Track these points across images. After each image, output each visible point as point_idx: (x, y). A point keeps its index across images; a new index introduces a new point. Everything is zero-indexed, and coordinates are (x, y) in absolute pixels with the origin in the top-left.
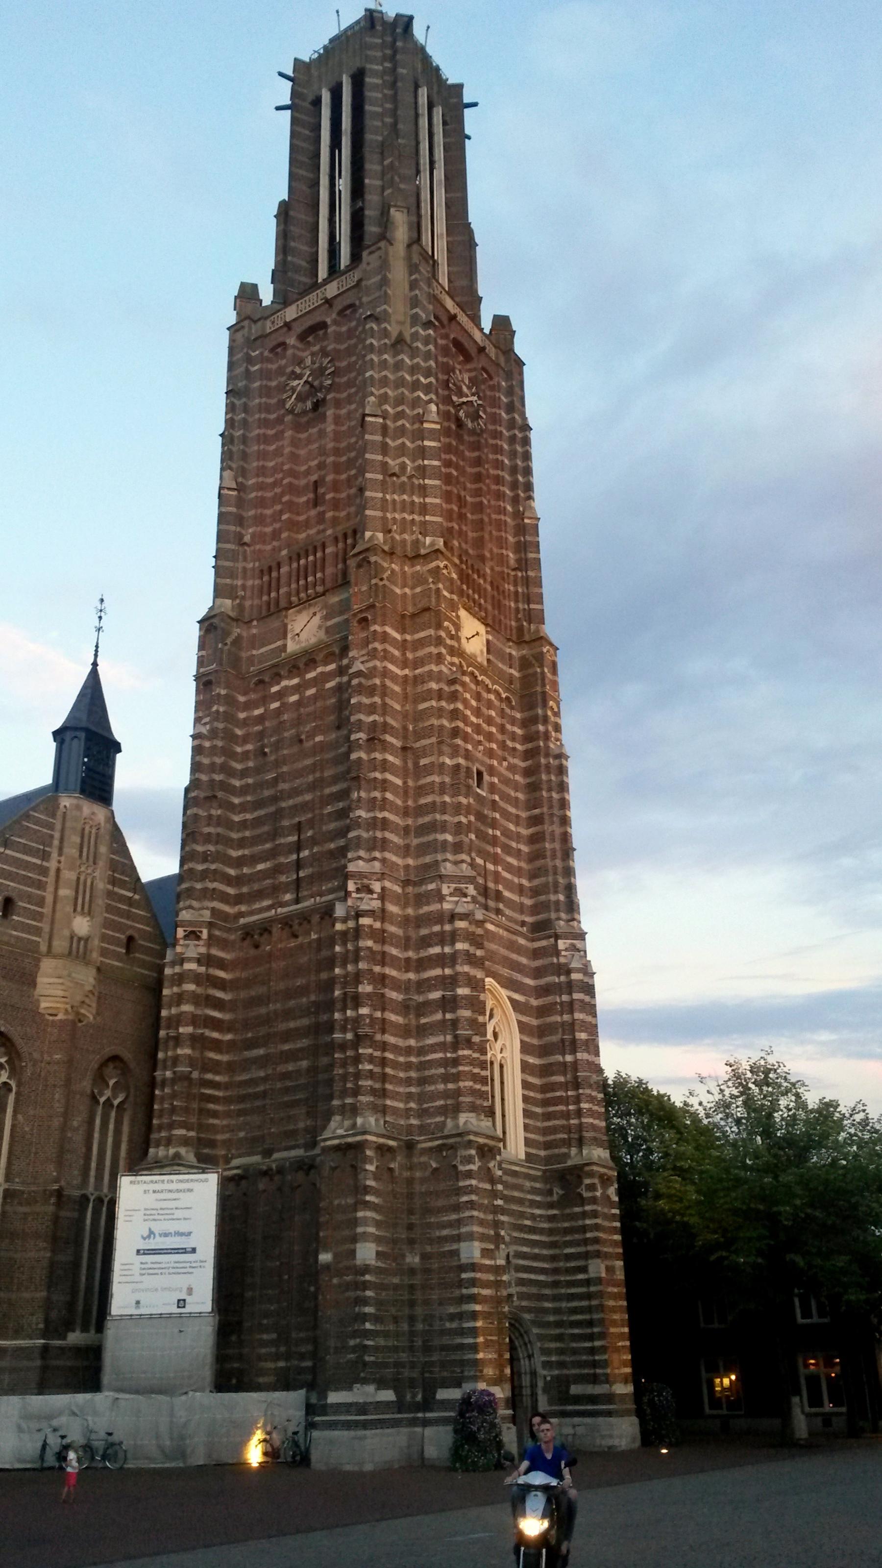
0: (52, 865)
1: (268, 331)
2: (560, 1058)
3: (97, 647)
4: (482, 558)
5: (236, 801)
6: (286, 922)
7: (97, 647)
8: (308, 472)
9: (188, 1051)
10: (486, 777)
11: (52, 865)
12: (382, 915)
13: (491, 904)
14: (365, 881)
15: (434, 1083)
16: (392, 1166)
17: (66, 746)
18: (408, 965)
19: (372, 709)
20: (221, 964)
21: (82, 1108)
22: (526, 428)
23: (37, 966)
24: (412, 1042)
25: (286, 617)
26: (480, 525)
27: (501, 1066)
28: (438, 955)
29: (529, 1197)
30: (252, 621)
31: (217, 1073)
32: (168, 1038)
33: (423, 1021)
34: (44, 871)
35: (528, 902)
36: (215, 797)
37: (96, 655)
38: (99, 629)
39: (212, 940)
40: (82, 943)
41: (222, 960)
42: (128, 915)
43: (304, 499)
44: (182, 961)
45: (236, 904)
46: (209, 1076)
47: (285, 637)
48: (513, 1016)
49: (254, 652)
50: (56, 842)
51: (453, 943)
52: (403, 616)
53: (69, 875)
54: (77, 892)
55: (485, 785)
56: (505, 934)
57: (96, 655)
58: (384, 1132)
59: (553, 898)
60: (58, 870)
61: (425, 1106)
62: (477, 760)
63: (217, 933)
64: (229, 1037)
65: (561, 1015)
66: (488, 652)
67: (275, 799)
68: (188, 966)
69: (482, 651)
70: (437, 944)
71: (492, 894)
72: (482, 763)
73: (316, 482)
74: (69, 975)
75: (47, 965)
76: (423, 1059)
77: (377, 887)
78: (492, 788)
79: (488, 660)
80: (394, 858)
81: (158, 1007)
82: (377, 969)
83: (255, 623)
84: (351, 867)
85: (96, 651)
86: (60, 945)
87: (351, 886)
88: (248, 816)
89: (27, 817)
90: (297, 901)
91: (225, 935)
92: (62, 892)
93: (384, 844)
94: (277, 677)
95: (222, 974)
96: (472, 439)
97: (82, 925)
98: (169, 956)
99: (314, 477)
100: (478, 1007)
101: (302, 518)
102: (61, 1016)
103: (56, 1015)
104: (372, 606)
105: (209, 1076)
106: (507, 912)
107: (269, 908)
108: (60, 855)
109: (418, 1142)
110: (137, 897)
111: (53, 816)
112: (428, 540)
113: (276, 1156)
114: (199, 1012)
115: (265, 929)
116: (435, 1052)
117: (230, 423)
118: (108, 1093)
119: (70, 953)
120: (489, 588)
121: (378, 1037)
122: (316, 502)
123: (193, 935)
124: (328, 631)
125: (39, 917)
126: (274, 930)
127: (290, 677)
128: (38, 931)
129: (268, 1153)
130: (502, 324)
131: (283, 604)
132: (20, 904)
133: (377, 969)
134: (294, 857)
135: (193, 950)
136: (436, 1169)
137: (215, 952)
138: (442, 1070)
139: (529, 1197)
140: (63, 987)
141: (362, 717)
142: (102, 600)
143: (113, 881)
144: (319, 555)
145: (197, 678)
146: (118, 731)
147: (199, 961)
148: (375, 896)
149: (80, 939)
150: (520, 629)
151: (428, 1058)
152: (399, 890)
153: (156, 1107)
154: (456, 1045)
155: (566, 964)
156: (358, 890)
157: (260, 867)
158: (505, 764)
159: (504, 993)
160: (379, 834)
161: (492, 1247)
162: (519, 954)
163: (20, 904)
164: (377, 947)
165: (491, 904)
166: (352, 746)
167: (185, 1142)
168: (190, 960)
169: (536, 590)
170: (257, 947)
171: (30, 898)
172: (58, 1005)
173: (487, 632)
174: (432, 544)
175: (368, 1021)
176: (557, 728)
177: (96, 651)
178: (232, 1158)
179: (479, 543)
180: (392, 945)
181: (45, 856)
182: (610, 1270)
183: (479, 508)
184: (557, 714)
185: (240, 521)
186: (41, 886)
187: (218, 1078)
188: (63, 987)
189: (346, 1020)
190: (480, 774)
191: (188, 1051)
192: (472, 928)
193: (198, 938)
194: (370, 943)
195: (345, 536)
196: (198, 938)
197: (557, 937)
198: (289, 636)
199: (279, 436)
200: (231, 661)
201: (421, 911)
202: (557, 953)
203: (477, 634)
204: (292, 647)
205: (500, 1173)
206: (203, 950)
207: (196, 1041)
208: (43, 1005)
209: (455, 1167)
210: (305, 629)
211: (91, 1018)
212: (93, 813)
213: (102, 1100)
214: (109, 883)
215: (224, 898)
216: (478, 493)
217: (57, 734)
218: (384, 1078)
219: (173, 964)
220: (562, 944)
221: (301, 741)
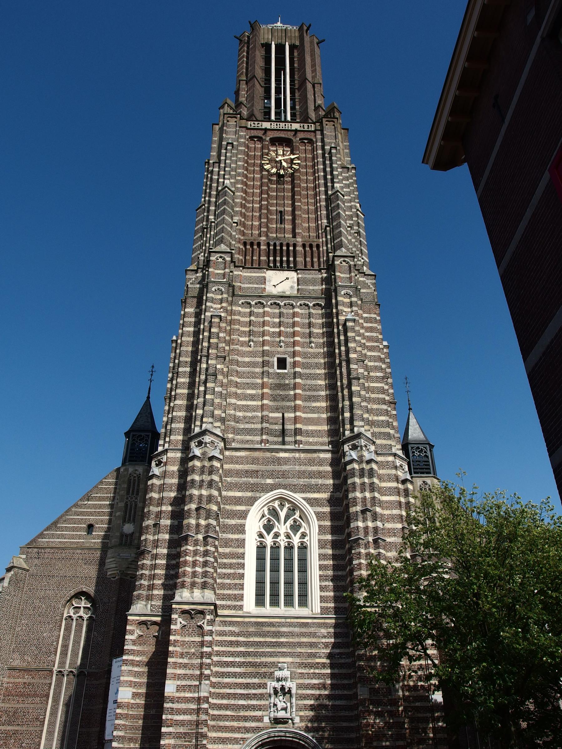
3: (150, 389)
7: (150, 389)
10: (289, 360)
29: (324, 640)
37: (149, 393)
54: (126, 512)
56: (302, 455)
57: (149, 393)
58: (149, 612)
74: (119, 555)
85: (149, 391)
89: (101, 482)
102: (117, 578)
132: (97, 526)
139: (324, 640)
140: (115, 562)
142: (153, 367)
149: (127, 536)
159: (298, 497)
161: (197, 683)
162: (321, 465)
163: (97, 526)
172: (115, 572)
173: (298, 274)
177: (149, 391)
188: (115, 562)
208: (109, 573)
212: (136, 470)
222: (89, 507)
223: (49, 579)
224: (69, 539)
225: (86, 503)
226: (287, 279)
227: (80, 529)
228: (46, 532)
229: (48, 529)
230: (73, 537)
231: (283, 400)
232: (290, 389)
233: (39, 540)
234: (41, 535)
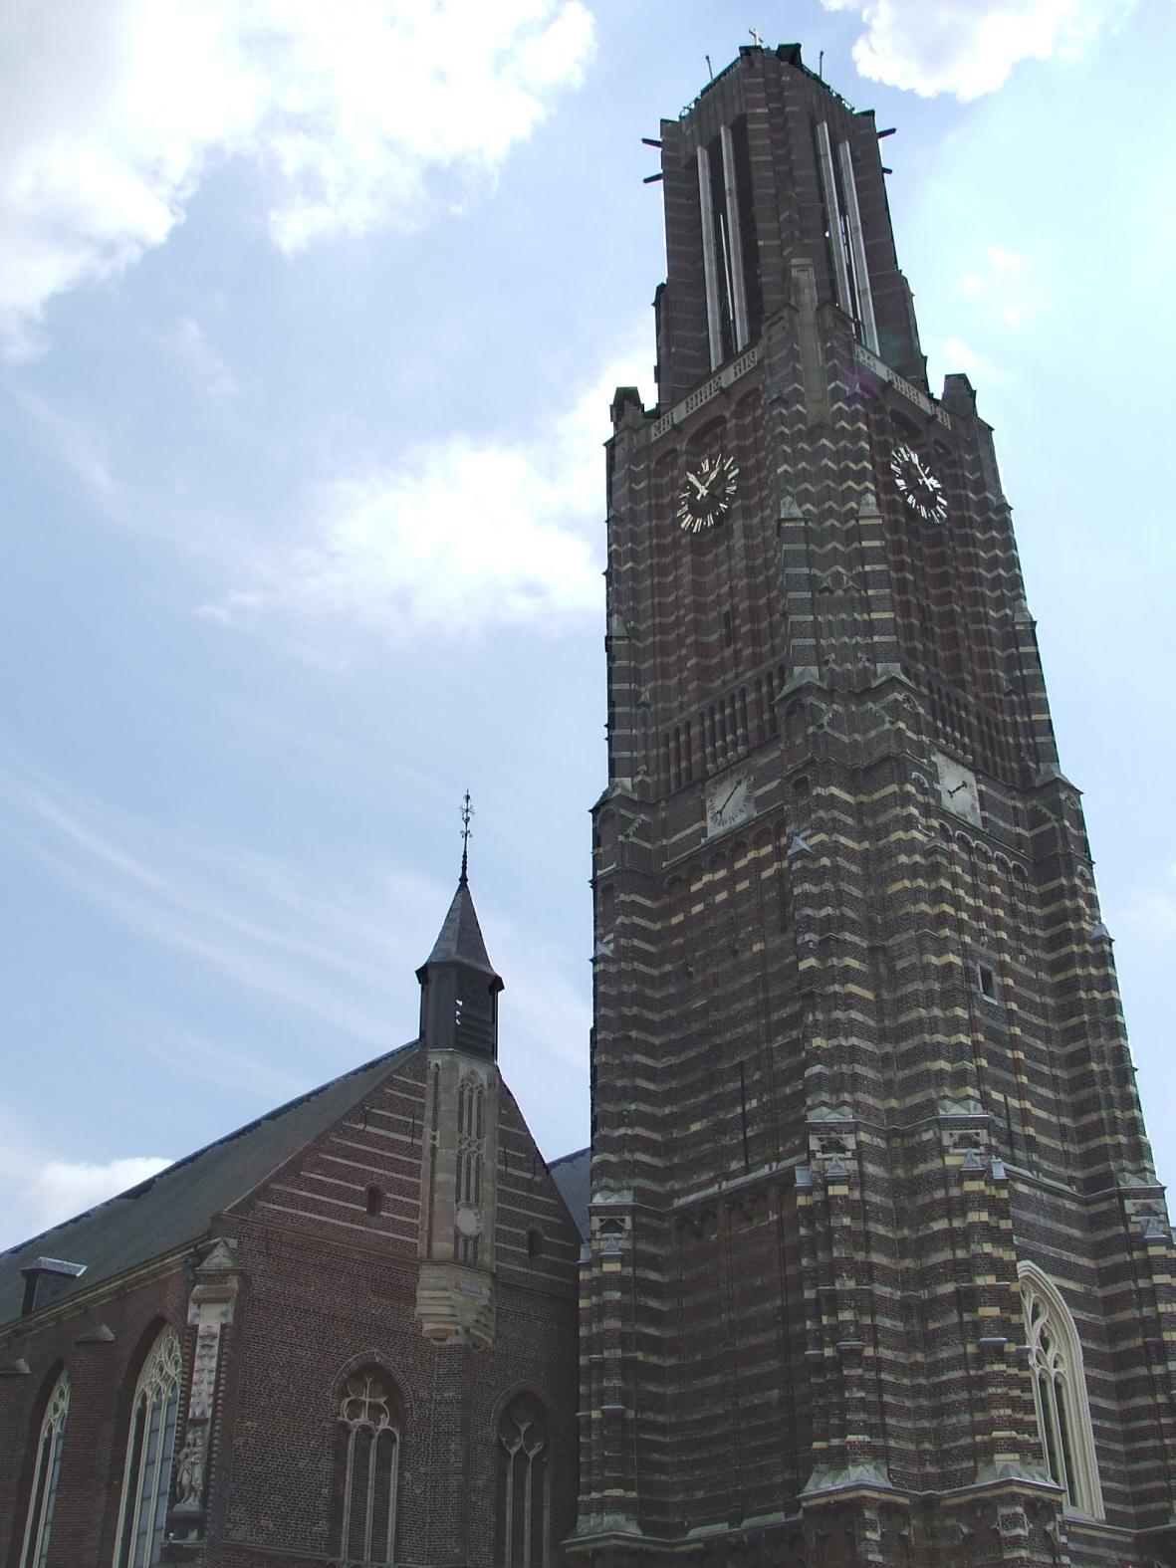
0: (426, 1142)
1: (654, 439)
2: (1142, 1371)
3: (465, 856)
4: (961, 684)
5: (657, 1041)
6: (734, 1198)
7: (465, 856)
8: (718, 602)
9: (616, 1383)
10: (996, 979)
11: (426, 1142)
12: (860, 1180)
13: (1020, 1154)
14: (833, 1135)
15: (956, 1413)
16: (905, 1533)
17: (432, 987)
18: (902, 1248)
19: (820, 901)
20: (654, 1263)
21: (487, 1463)
22: (1005, 508)
23: (416, 1275)
24: (919, 1357)
25: (703, 790)
26: (952, 640)
27: (1058, 1387)
28: (944, 1232)
30: (659, 802)
31: (661, 1411)
32: (592, 1365)
33: (932, 1325)
34: (416, 1152)
35: (1074, 1149)
36: (629, 1038)
37: (464, 868)
39: (638, 1232)
40: (471, 1243)
41: (654, 1257)
42: (528, 1204)
43: (714, 637)
44: (599, 1260)
45: (668, 1179)
46: (650, 1416)
47: (703, 818)
48: (1068, 1314)
49: (665, 842)
50: (429, 1114)
51: (964, 1215)
52: (855, 772)
53: (447, 1155)
56: (1045, 1196)
57: (464, 868)
59: (1108, 1140)
60: (434, 1148)
61: (945, 1446)
62: (981, 956)
63: (644, 1220)
64: (671, 1361)
65: (1140, 1308)
66: (982, 809)
67: (704, 1035)
68: (608, 1267)
69: (973, 807)
70: (941, 1217)
72: (989, 960)
73: (727, 614)
75: (427, 1275)
76: (937, 1380)
77: (850, 1142)
78: (1007, 993)
79: (984, 819)
80: (871, 1101)
82: (860, 1256)
83: (663, 804)
84: (813, 1117)
85: (465, 862)
86: (443, 1247)
87: (814, 1144)
88: (674, 1060)
89: (391, 1082)
90: (747, 1170)
91: (656, 1223)
92: (440, 1177)
93: (855, 1082)
94: (695, 873)
95: (654, 1276)
96: (930, 532)
97: (468, 1221)
98: (584, 1255)
99: (726, 608)
100: (1013, 1303)
101: (714, 661)
102: (451, 1341)
103: (444, 1340)
104: (812, 762)
105: (650, 1416)
106: (1046, 1165)
107: (710, 1183)
108: (434, 1129)
109: (941, 1498)
110: (538, 1179)
111: (423, 1077)
112: (880, 667)
113: (747, 1523)
114: (627, 1329)
115: (706, 1211)
116: (954, 1368)
117: (612, 557)
118: (520, 1442)
119: (456, 1257)
120: (974, 721)
121: (869, 1351)
122: (729, 639)
123: (612, 1226)
124: (760, 802)
125: (415, 1211)
126: (720, 1212)
127: (713, 870)
128: (412, 1230)
129: (735, 1521)
130: (960, 387)
131: (697, 774)
132: (388, 1195)
133: (860, 1256)
134: (739, 1110)
135: (613, 1244)
136: (971, 1536)
137: (643, 1246)
138: (965, 1395)
141: (808, 911)
142: (468, 797)
143: (506, 1160)
144: (738, 705)
145: (594, 883)
146: (498, 965)
148: (849, 1154)
149: (467, 1239)
150: (1025, 771)
151: (944, 1378)
152: (883, 1144)
153: (582, 1459)
154: (980, 1360)
155: (1141, 1235)
156: (824, 1150)
157: (695, 1127)
158: (1022, 958)
159: (1051, 1281)
160: (845, 1068)
163: (388, 1195)
164: (857, 1226)
165: (1020, 1154)
167: (621, 1505)
168: (611, 1259)
170: (699, 1235)
171: (401, 1188)
172: (446, 1326)
173: (978, 781)
174: (886, 672)
175: (852, 1330)
176: (1093, 902)
177: (465, 862)
178: (689, 1528)
179: (955, 665)
180: (878, 1221)
181: (416, 1132)
183: (949, 618)
184: (1090, 883)
185: (635, 676)
186: (414, 1170)
187: (661, 1418)
189: (822, 1329)
190: (986, 976)
191: (616, 1383)
192: (991, 1191)
194: (847, 1221)
195: (770, 677)
196: (620, 1229)
197: (1123, 1195)
198: (709, 815)
199: (676, 563)
200: (637, 857)
201: (916, 1172)
202: (1125, 1219)
203: (964, 784)
204: (714, 830)
205: (1063, 1539)
206: (626, 1245)
207: (627, 1367)
208: (427, 1327)
209: (996, 1532)
210: (729, 807)
211: (490, 1341)
212: (473, 1072)
213: (513, 1451)
214: (500, 1162)
215: (650, 1172)
216: (946, 598)
217: (422, 974)
218: (883, 1409)
219: (588, 1266)
220: (1129, 1206)
221: (735, 953)
222: (362, 1137)
223: (299, 1319)
224: (329, 1215)
225: (361, 1126)
226: (964, 784)
227: (351, 1196)
228: (277, 1187)
229: (278, 1178)
230: (317, 1207)
231: (1001, 1067)
232: (1003, 1045)
233: (261, 1204)
234: (264, 1192)
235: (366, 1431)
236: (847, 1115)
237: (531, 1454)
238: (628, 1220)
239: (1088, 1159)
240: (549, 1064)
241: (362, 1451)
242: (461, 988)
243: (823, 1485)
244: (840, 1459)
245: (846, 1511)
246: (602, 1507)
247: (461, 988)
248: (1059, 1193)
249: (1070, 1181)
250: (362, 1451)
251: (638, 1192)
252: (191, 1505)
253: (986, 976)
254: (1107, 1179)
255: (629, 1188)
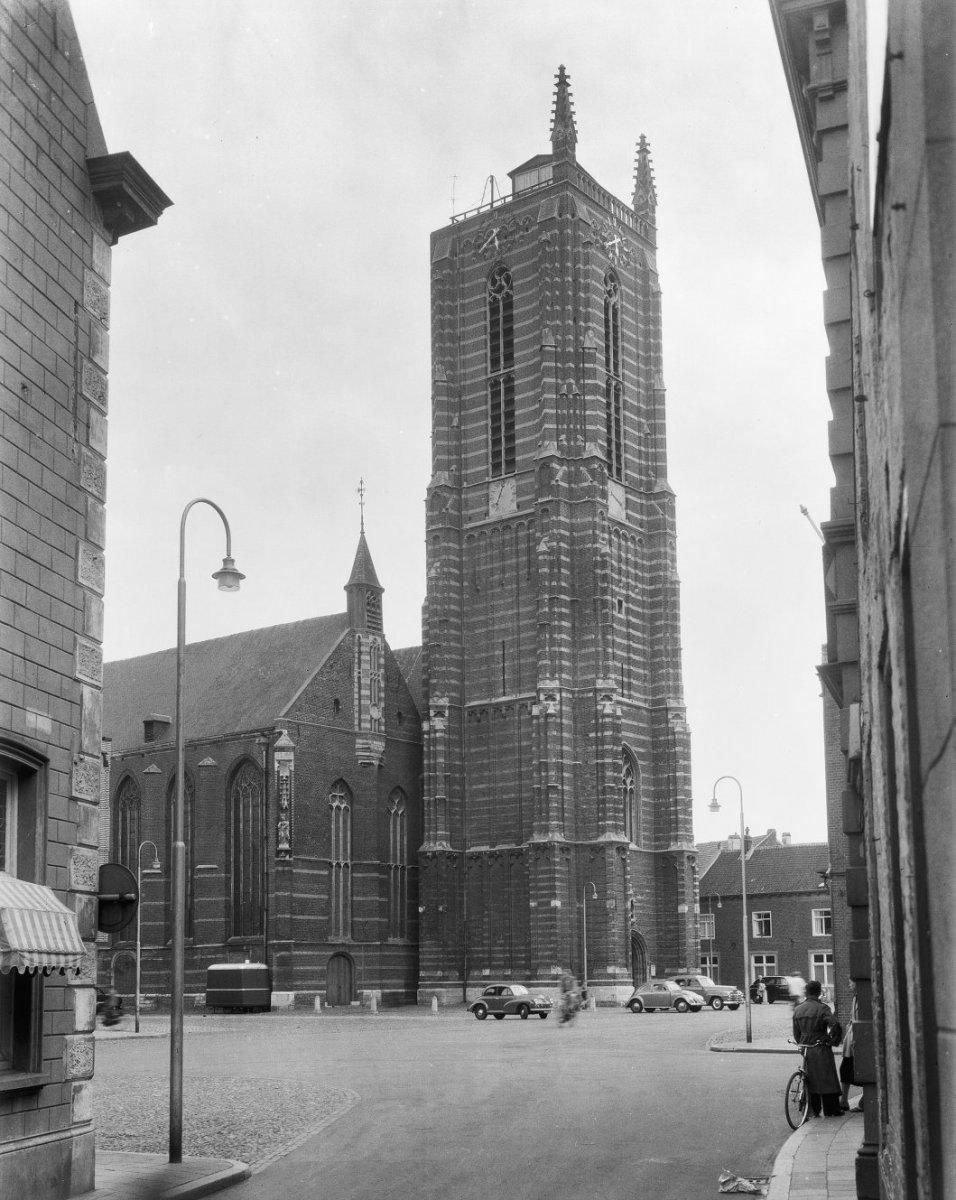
10: (624, 604)
13: (625, 692)
38: (361, 504)
51: (602, 731)
55: (623, 610)
68: (438, 735)
71: (626, 672)
77: (558, 697)
81: (422, 761)
84: (541, 685)
92: (363, 692)
93: (561, 669)
113: (497, 848)
123: (440, 714)
129: (493, 846)
147: (444, 731)
165: (625, 692)
166: (539, 604)
169: (662, 436)
176: (674, 560)
182: (691, 909)
184: (674, 549)
190: (620, 602)
193: (443, 716)
196: (443, 716)
198: (490, 503)
200: (449, 517)
204: (494, 515)
213: (393, 812)
235: (338, 808)
236: (556, 684)
237: (400, 812)
238: (447, 712)
239: (655, 691)
240: (403, 626)
241: (337, 816)
242: (365, 590)
243: (538, 839)
244: (546, 830)
245: (546, 848)
246: (436, 839)
247: (365, 590)
248: (639, 708)
249: (645, 701)
250: (337, 816)
251: (451, 699)
252: (285, 846)
253: (620, 602)
254: (662, 701)
255: (447, 696)
